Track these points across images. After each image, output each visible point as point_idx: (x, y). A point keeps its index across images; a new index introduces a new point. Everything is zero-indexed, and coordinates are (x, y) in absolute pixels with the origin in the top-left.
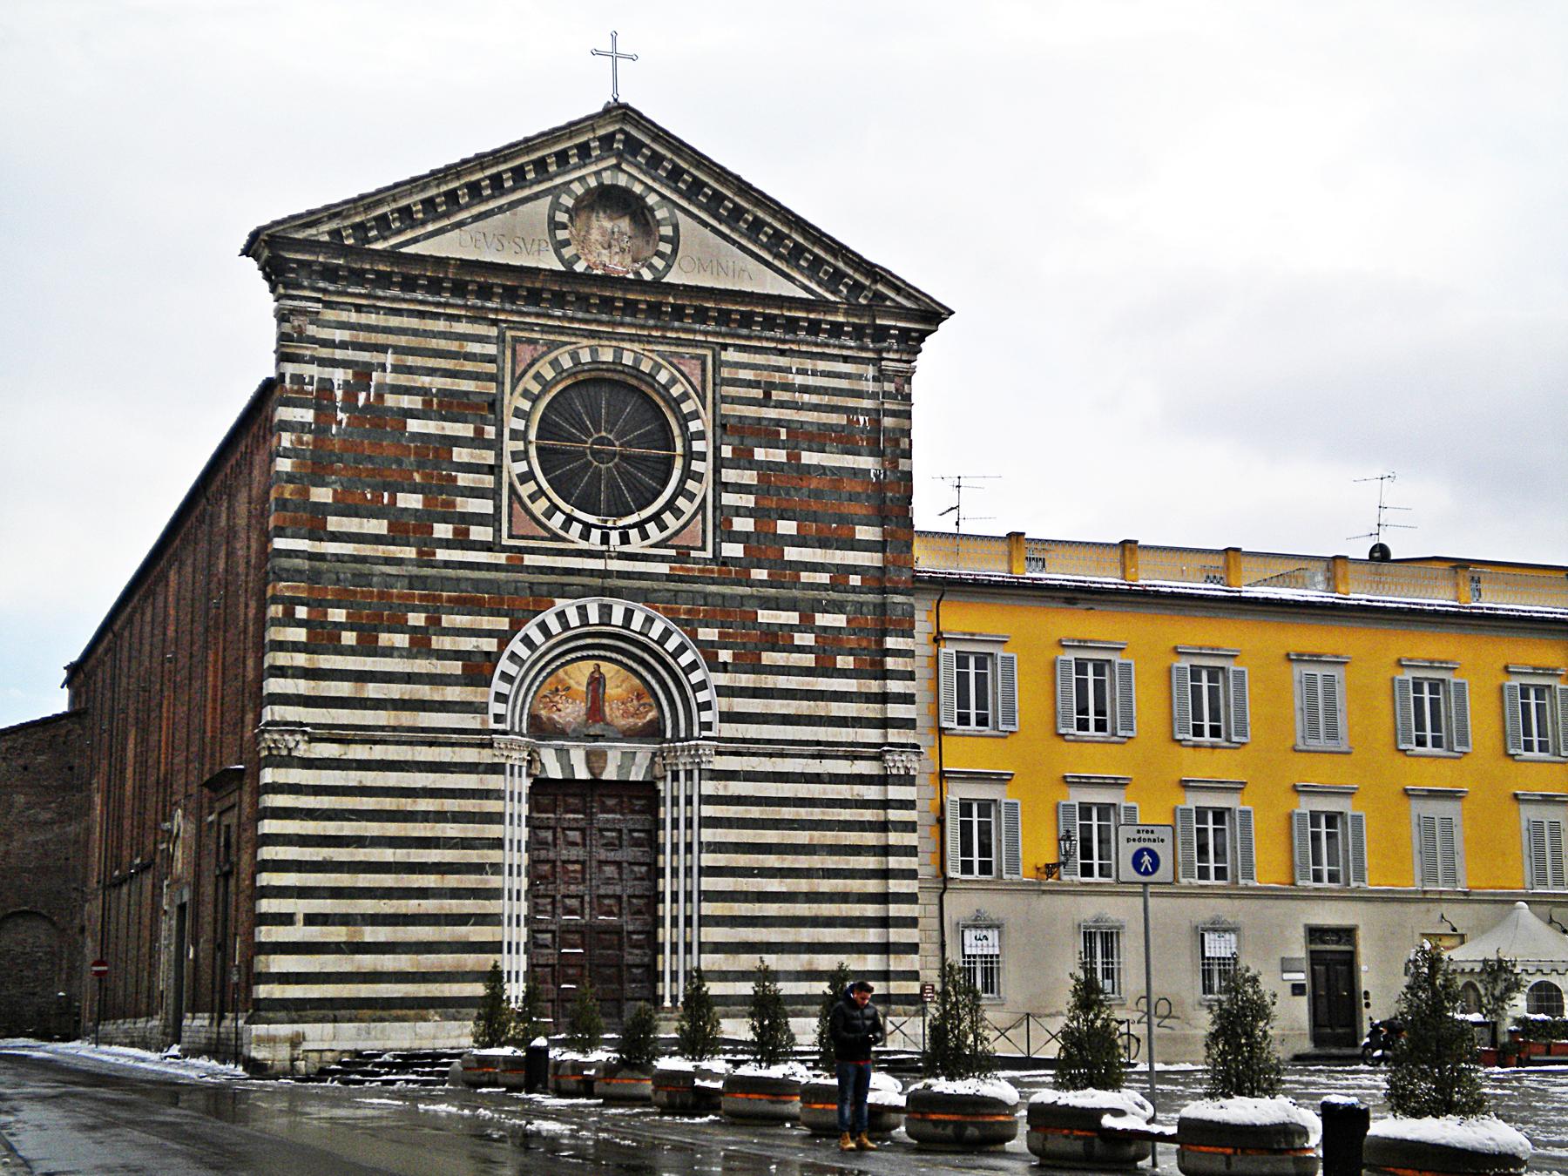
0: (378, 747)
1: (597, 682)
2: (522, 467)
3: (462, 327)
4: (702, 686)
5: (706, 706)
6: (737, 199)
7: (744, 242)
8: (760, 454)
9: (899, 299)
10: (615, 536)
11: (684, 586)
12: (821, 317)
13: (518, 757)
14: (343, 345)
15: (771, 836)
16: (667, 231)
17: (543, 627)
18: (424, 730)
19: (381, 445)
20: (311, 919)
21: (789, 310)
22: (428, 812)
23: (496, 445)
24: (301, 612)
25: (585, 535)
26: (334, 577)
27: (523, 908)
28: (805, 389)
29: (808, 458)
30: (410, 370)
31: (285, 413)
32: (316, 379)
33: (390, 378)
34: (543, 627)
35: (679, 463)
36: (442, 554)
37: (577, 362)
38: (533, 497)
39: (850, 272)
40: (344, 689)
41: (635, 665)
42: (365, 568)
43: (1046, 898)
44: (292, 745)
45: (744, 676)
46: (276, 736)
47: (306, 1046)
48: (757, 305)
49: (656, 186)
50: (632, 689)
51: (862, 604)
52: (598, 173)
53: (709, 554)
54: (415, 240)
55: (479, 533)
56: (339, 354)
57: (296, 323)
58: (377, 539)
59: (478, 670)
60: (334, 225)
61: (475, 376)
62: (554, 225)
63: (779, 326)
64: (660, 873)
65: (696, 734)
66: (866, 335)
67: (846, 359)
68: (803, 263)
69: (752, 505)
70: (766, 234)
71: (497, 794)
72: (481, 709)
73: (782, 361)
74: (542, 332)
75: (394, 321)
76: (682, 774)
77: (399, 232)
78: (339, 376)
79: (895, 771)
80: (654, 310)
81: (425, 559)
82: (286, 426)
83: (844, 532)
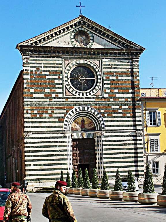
1: (83, 121)
2: (67, 83)
5: (103, 124)
6: (104, 31)
7: (106, 39)
8: (111, 78)
9: (135, 47)
10: (85, 94)
11: (97, 103)
13: (69, 135)
14: (34, 63)
16: (92, 38)
17: (73, 112)
18: (52, 131)
19: (42, 81)
20: (34, 165)
21: (115, 51)
22: (53, 146)
23: (62, 79)
24: (29, 112)
25: (79, 95)
26: (35, 105)
27: (71, 162)
29: (120, 78)
30: (46, 67)
31: (25, 77)
32: (30, 70)
34: (73, 112)
35: (96, 80)
36: (54, 100)
38: (69, 88)
39: (126, 43)
41: (90, 118)
44: (29, 135)
46: (26, 134)
47: (34, 187)
49: (89, 30)
50: (90, 122)
53: (102, 97)
54: (46, 44)
56: (34, 65)
57: (26, 60)
58: (42, 98)
59: (61, 120)
61: (58, 67)
63: (113, 54)
64: (96, 154)
65: (101, 129)
68: (117, 42)
69: (110, 87)
70: (110, 37)
71: (66, 142)
72: (61, 127)
75: (43, 59)
76: (99, 137)
77: (43, 42)
78: (34, 69)
79: (138, 134)
80: (90, 53)
82: (25, 79)
83: (127, 91)
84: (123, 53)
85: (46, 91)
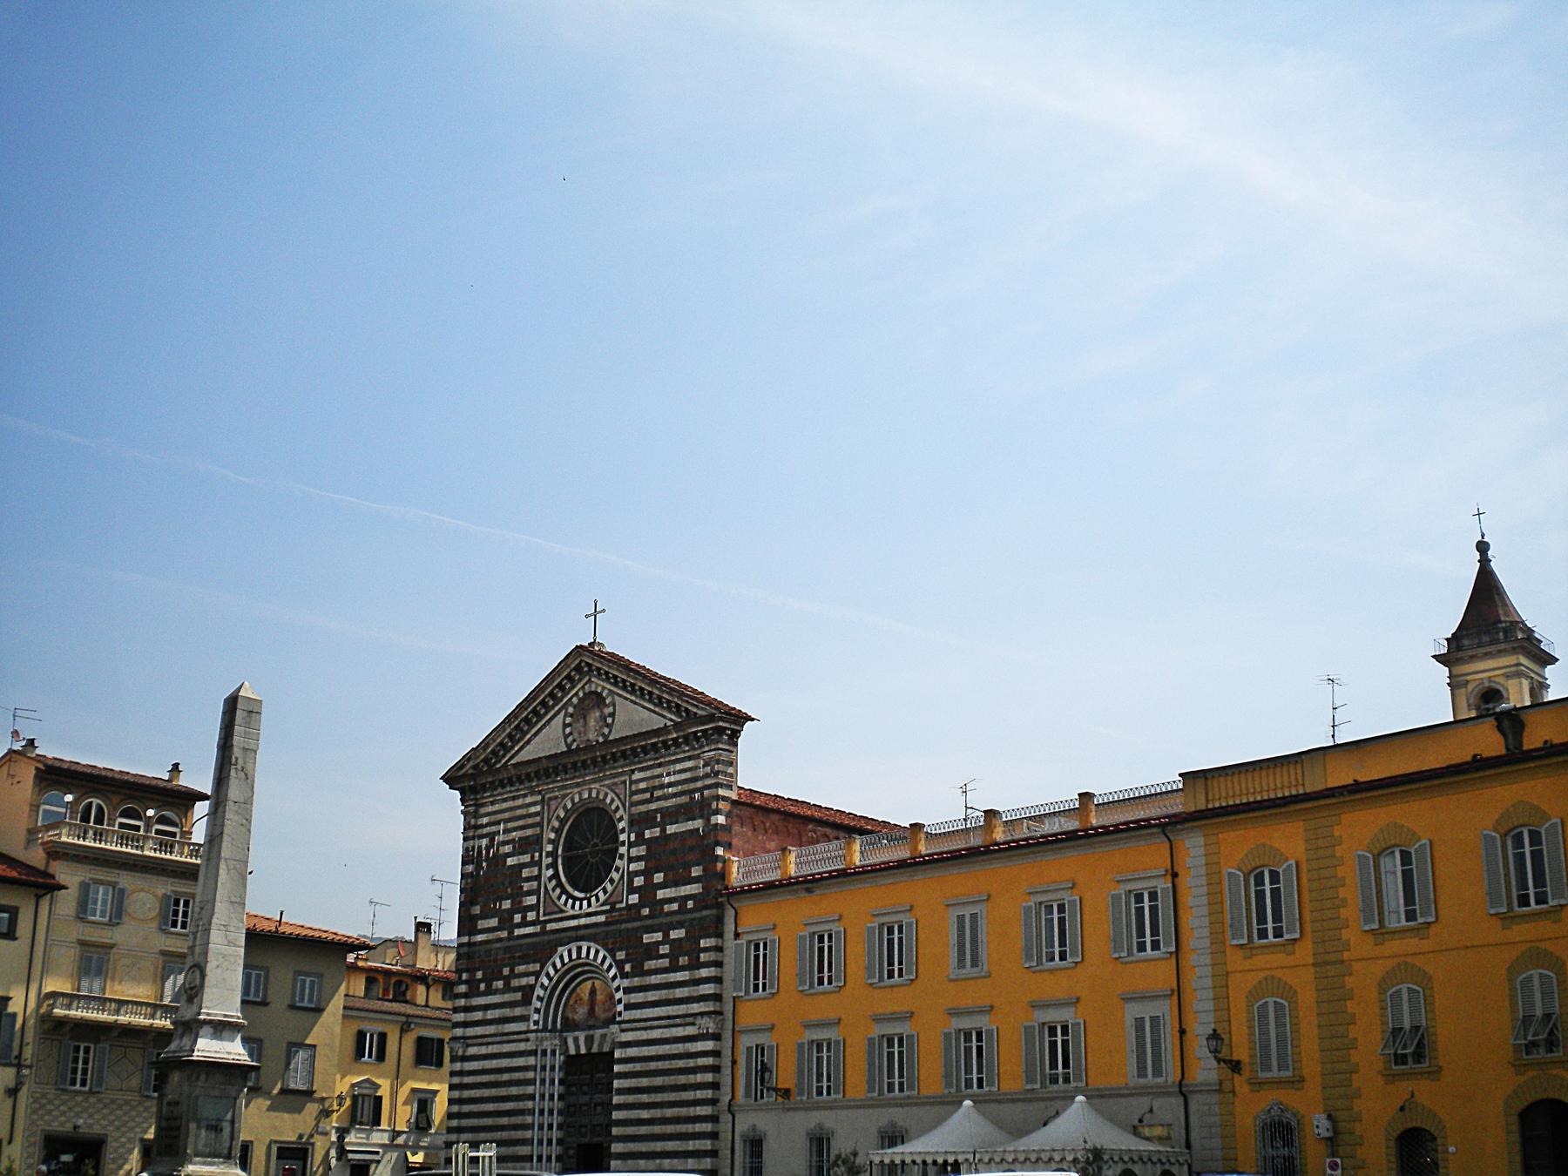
0: (490, 1047)
1: (593, 992)
3: (529, 800)
4: (618, 989)
5: (620, 1001)
10: (585, 902)
12: (664, 738)
15: (645, 1082)
23: (539, 864)
24: (464, 976)
25: (573, 907)
28: (670, 785)
29: (671, 829)
33: (502, 838)
34: (554, 965)
36: (517, 932)
37: (573, 804)
38: (554, 890)
40: (478, 1016)
42: (488, 946)
43: (791, 1114)
45: (636, 979)
48: (635, 742)
51: (694, 919)
52: (583, 687)
53: (624, 905)
55: (531, 916)
56: (485, 831)
60: (471, 763)
62: (565, 726)
63: (650, 750)
66: (681, 743)
67: (689, 758)
73: (658, 771)
74: (558, 791)
77: (504, 756)
78: (484, 842)
81: (511, 937)
84: (673, 739)
85: (503, 907)
